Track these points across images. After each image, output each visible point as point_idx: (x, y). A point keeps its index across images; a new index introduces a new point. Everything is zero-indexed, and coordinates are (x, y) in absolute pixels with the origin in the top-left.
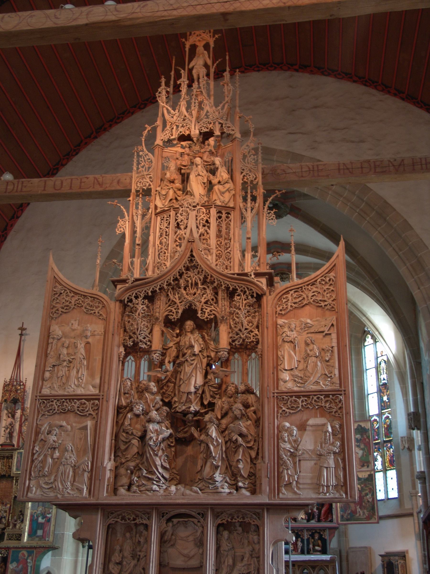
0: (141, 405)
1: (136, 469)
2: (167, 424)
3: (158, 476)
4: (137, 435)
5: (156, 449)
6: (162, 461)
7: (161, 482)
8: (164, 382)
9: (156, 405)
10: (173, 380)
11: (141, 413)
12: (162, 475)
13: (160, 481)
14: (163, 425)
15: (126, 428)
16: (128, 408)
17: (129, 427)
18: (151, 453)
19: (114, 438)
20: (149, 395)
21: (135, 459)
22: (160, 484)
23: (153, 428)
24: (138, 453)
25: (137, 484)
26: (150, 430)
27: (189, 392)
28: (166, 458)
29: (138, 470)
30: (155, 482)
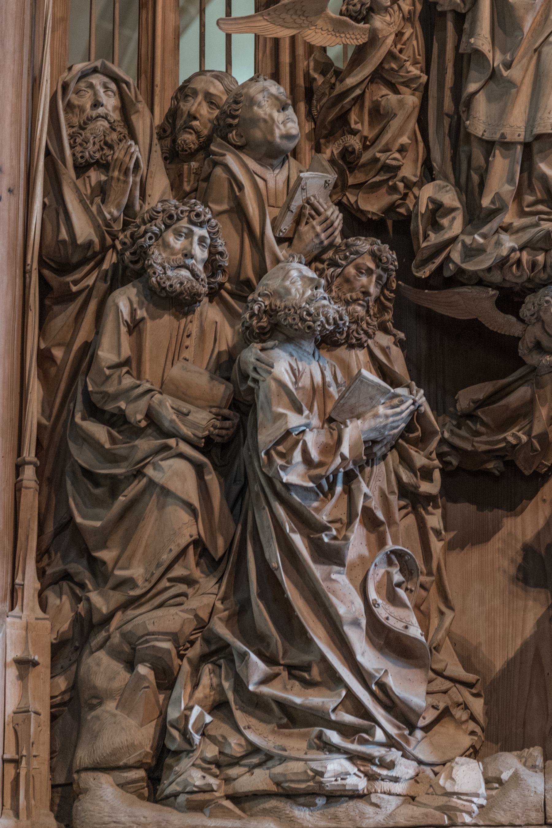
0: (203, 232)
1: (194, 652)
2: (385, 351)
3: (350, 694)
4: (186, 431)
5: (324, 518)
6: (373, 595)
7: (379, 735)
8: (350, 81)
9: (303, 228)
10: (415, 71)
11: (204, 290)
12: (382, 686)
13: (370, 731)
14: (362, 355)
15: (111, 388)
16: (111, 258)
17: (128, 381)
18: (297, 539)
19: (29, 454)
20: (253, 165)
21: (182, 588)
22: (376, 752)
23: (296, 374)
24: (197, 543)
25: (211, 751)
26: (281, 384)
27: (539, 137)
28: (397, 577)
29: (204, 658)
30: (334, 737)
